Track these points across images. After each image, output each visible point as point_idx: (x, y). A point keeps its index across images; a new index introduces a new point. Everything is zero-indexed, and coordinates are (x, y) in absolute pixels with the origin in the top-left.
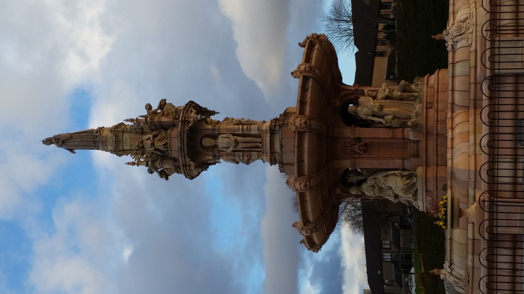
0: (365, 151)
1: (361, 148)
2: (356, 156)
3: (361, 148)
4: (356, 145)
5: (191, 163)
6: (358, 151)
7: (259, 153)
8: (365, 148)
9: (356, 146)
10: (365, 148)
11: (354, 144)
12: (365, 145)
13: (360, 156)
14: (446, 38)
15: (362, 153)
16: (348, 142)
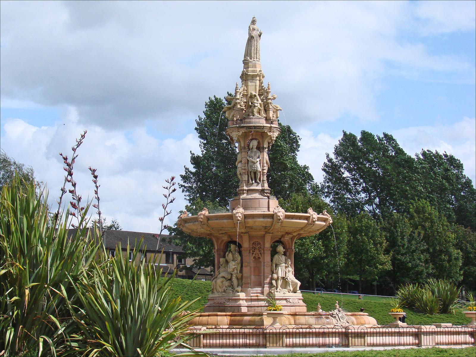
0: (254, 257)
1: (257, 255)
2: (251, 251)
3: (257, 255)
4: (259, 251)
5: (241, 132)
6: (255, 253)
7: (247, 181)
8: (257, 258)
9: (258, 251)
10: (257, 258)
11: (260, 250)
12: (259, 258)
13: (251, 254)
14: (336, 311)
15: (254, 255)
16: (261, 246)
